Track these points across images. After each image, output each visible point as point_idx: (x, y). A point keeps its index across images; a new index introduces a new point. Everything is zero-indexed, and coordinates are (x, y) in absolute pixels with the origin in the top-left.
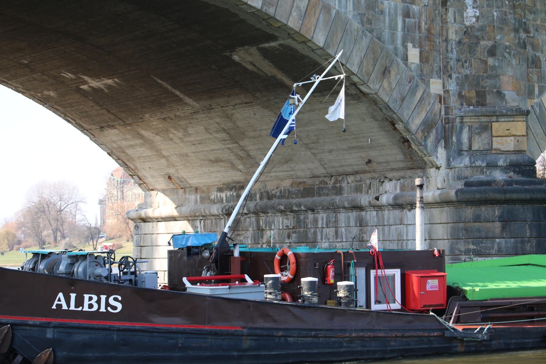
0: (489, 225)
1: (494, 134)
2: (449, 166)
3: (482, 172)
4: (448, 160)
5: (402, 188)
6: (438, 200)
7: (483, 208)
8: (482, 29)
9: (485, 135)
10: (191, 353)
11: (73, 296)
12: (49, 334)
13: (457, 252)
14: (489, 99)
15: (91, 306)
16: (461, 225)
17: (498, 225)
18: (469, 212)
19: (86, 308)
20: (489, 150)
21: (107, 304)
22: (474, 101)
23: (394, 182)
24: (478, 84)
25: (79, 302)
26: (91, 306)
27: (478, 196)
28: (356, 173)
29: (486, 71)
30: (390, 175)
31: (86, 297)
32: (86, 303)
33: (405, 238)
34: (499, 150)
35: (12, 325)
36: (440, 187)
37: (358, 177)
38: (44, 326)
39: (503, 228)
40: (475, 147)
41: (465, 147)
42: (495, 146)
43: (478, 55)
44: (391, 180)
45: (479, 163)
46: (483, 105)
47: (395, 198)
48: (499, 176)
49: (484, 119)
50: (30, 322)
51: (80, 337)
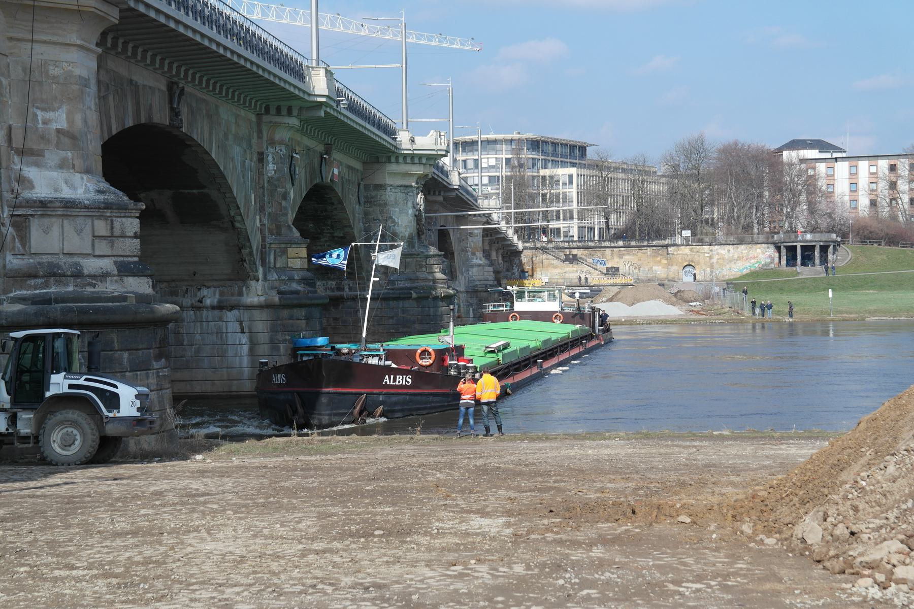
0: (299, 322)
1: (289, 256)
2: (265, 279)
3: (286, 284)
4: (265, 275)
5: (221, 294)
6: (263, 304)
7: (295, 310)
8: (278, 180)
9: (284, 257)
10: (433, 405)
11: (392, 376)
12: (381, 398)
13: (276, 341)
14: (284, 230)
15: (399, 382)
16: (279, 322)
17: (304, 321)
18: (285, 313)
19: (397, 383)
20: (285, 269)
21: (406, 381)
22: (274, 231)
23: (212, 289)
25: (395, 380)
26: (399, 382)
27: (295, 302)
28: (173, 281)
30: (207, 284)
31: (398, 377)
32: (398, 380)
33: (225, 331)
34: (292, 268)
35: (367, 394)
36: (260, 294)
37: (173, 284)
39: (307, 323)
40: (278, 266)
41: (272, 266)
42: (289, 264)
44: (209, 288)
45: (283, 277)
46: (280, 235)
47: (220, 301)
48: (295, 286)
49: (283, 246)
51: (394, 399)
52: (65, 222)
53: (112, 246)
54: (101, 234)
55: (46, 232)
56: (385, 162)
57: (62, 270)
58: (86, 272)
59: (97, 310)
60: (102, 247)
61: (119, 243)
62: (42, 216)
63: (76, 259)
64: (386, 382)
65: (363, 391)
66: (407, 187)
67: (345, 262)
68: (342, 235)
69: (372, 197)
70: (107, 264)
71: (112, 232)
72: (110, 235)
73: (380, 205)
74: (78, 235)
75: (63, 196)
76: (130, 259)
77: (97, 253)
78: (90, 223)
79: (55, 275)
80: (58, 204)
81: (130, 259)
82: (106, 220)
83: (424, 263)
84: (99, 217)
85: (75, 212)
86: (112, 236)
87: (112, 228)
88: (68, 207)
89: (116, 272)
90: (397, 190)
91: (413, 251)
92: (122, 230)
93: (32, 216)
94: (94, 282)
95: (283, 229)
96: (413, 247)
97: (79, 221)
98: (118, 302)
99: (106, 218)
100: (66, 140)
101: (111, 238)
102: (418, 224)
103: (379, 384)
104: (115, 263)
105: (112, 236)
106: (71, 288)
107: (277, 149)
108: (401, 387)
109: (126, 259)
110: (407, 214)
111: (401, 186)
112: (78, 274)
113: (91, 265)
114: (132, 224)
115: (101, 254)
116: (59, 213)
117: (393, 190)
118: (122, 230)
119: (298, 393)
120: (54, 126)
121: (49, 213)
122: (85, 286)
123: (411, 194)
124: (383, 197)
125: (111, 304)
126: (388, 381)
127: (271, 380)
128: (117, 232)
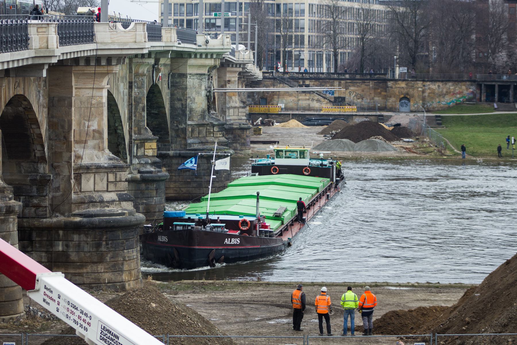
1: (146, 148)
3: (143, 166)
9: (143, 149)
11: (229, 239)
13: (137, 204)
14: (143, 131)
18: (143, 186)
19: (232, 243)
21: (237, 241)
24: (138, 124)
25: (231, 241)
29: (141, 119)
31: (232, 239)
32: (232, 241)
35: (216, 249)
38: (222, 249)
40: (139, 154)
43: (138, 110)
45: (142, 162)
50: (220, 248)
52: (96, 175)
53: (116, 186)
54: (111, 181)
55: (88, 181)
56: (187, 58)
57: (95, 199)
58: (105, 200)
59: (114, 221)
60: (111, 187)
61: (119, 184)
62: (86, 173)
63: (100, 193)
64: (226, 243)
65: (213, 248)
66: (201, 75)
67: (196, 165)
68: (157, 112)
69: (177, 83)
70: (113, 196)
71: (116, 179)
72: (114, 181)
73: (182, 89)
74: (102, 181)
75: (95, 162)
76: (123, 192)
77: (109, 190)
78: (106, 176)
79: (92, 202)
80: (93, 167)
81: (123, 192)
82: (114, 173)
83: (212, 131)
84: (111, 172)
85: (101, 170)
86: (116, 181)
87: (116, 177)
88: (98, 168)
89: (118, 200)
90: (195, 77)
91: (204, 122)
92: (120, 178)
93: (82, 173)
94: (108, 205)
95: (142, 131)
96: (204, 119)
97: (102, 174)
98: (122, 216)
99: (113, 173)
100: (97, 135)
101: (115, 182)
102: (208, 102)
103: (222, 243)
104: (117, 195)
105: (116, 181)
106: (98, 209)
107: (140, 79)
108: (234, 245)
109: (121, 192)
110: (201, 95)
111: (197, 74)
112: (102, 202)
113: (108, 196)
114: (124, 175)
115: (111, 190)
116: (94, 171)
117: (192, 77)
118: (120, 178)
119: (176, 248)
120: (92, 128)
121: (90, 172)
122: (104, 207)
123: (204, 80)
124: (184, 83)
125: (118, 217)
126: (227, 242)
127: (157, 238)
128: (118, 179)
